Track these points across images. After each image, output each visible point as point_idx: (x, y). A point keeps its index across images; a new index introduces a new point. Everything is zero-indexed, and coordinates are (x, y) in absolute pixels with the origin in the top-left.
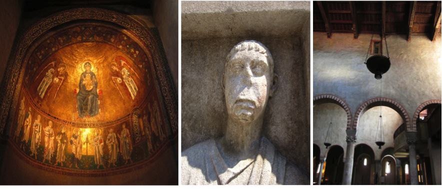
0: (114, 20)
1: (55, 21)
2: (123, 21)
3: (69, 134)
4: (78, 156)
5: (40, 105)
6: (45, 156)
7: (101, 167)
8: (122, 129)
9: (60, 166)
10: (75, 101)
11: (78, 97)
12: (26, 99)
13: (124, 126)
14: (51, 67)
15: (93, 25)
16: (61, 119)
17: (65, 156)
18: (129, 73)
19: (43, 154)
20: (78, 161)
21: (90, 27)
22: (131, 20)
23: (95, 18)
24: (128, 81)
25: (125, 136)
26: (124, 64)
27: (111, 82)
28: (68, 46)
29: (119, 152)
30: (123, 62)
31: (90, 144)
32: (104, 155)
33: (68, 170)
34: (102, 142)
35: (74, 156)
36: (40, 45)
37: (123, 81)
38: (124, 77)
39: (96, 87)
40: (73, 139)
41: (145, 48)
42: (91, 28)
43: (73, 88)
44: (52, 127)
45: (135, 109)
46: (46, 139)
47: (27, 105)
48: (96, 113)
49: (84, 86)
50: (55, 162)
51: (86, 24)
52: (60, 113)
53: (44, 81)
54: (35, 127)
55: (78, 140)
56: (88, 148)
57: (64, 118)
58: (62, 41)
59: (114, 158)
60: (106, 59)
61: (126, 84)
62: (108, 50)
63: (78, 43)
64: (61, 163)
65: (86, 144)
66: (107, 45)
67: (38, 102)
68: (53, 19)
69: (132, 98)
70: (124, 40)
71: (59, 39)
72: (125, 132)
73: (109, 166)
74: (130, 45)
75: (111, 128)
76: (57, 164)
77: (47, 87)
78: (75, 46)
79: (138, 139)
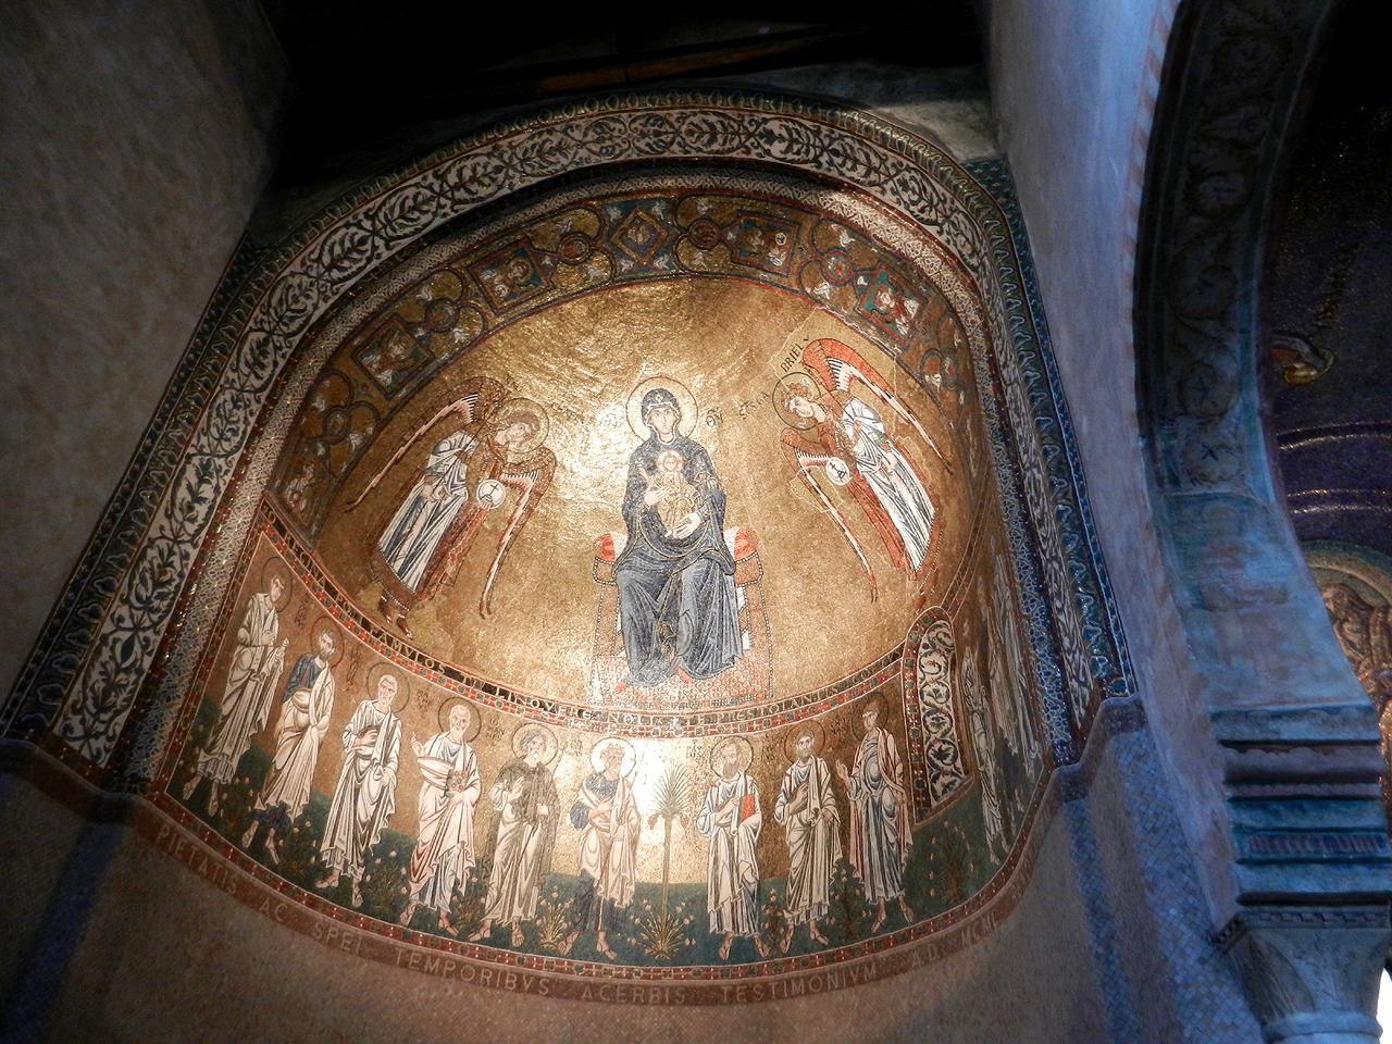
0: (777, 149)
1: (456, 187)
2: (824, 149)
3: (565, 773)
4: (616, 892)
5: (401, 624)
6: (415, 888)
7: (743, 949)
8: (861, 734)
9: (507, 945)
10: (609, 601)
11: (625, 576)
12: (291, 588)
13: (870, 718)
14: (453, 422)
15: (669, 190)
16: (524, 691)
17: (535, 891)
18: (880, 427)
19: (405, 881)
20: (615, 920)
21: (652, 201)
22: (864, 136)
23: (676, 151)
24: (884, 470)
25: (873, 770)
27: (796, 486)
28: (537, 311)
29: (845, 860)
30: (845, 372)
31: (684, 822)
33: (549, 966)
35: (592, 890)
36: (374, 315)
38: (859, 449)
39: (720, 520)
40: (587, 798)
41: (948, 274)
42: (657, 209)
43: (593, 533)
45: (929, 622)
46: (428, 799)
47: (298, 621)
49: (652, 516)
50: (475, 926)
51: (628, 187)
52: (518, 663)
54: (362, 734)
55: (618, 801)
56: (673, 846)
57: (543, 686)
60: (754, 361)
61: (877, 490)
62: (758, 313)
63: (594, 289)
65: (661, 821)
66: (755, 289)
67: (383, 608)
68: (441, 177)
69: (909, 559)
70: (837, 250)
71: (486, 277)
72: (877, 747)
73: (785, 946)
74: (871, 274)
75: (805, 729)
77: (441, 528)
78: (578, 309)
79: (946, 787)
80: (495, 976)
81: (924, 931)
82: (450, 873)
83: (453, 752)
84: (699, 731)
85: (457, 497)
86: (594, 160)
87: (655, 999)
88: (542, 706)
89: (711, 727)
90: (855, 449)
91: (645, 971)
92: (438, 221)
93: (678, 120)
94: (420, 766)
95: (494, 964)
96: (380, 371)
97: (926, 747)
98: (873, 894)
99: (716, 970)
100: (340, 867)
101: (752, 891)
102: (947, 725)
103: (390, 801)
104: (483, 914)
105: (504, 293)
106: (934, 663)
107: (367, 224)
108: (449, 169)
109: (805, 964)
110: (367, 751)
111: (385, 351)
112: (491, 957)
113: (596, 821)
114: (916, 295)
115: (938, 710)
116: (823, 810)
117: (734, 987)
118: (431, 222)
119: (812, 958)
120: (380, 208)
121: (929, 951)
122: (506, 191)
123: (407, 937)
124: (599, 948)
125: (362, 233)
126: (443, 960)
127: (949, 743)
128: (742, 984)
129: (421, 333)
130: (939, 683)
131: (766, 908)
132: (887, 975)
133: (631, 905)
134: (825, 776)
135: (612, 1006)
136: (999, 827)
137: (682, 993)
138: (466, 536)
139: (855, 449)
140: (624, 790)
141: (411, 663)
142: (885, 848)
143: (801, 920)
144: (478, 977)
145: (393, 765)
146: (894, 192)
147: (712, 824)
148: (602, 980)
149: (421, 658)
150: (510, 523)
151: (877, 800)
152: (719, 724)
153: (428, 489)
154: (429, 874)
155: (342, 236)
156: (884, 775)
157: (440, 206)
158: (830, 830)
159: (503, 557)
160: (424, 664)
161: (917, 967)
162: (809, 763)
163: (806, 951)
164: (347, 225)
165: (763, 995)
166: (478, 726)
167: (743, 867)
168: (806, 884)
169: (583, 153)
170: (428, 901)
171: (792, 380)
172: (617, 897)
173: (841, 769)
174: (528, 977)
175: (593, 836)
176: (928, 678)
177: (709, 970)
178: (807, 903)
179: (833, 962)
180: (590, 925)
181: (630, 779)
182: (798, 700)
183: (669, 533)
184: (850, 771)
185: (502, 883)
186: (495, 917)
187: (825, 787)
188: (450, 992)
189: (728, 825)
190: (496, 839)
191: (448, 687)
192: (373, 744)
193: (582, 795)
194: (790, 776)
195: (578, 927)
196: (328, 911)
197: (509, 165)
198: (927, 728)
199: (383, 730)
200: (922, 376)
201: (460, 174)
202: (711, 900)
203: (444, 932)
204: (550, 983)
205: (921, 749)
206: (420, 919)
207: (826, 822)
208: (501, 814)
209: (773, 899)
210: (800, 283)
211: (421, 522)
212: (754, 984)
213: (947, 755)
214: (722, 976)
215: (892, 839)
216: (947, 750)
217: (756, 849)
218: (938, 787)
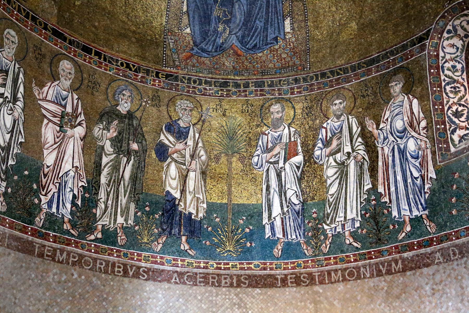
8: (388, 98)
9: (114, 243)
19: (36, 194)
25: (399, 125)
31: (242, 159)
32: (303, 203)
34: (297, 154)
44: (73, 89)
48: (271, 36)
50: (90, 229)
55: (190, 142)
80: (107, 265)
81: (448, 238)
82: (69, 190)
83: (64, 97)
87: (226, 283)
88: (128, 66)
89: (261, 90)
91: (217, 264)
94: (41, 106)
95: (106, 257)
97: (446, 108)
98: (399, 212)
99: (271, 264)
101: (297, 211)
102: (462, 93)
103: (20, 131)
106: (453, 46)
109: (342, 260)
112: (103, 251)
113: (175, 156)
115: (455, 81)
116: (355, 154)
117: (286, 275)
119: (347, 256)
121: (451, 253)
124: (182, 247)
127: (464, 106)
128: (292, 274)
130: (456, 61)
131: (309, 222)
132: (411, 269)
134: (356, 129)
135: (195, 288)
137: (246, 279)
140: (194, 135)
141: (27, 22)
142: (409, 180)
143: (338, 230)
144: (95, 265)
145: (20, 104)
147: (264, 161)
148: (186, 270)
149: (34, 19)
151: (402, 147)
152: (266, 88)
154: (53, 189)
156: (409, 128)
158: (361, 167)
160: (36, 24)
162: (342, 118)
163: (342, 252)
165: (308, 282)
166: (81, 79)
167: (290, 193)
170: (54, 210)
172: (194, 212)
173: (371, 126)
174: (132, 267)
175: (173, 167)
176: (448, 57)
177: (265, 264)
178: (343, 219)
179: (365, 259)
180: (175, 231)
181: (199, 126)
184: (378, 125)
185: (108, 199)
186: (104, 223)
187: (355, 137)
188: (76, 276)
189: (277, 162)
190: (101, 165)
191: (56, 45)
193: (162, 137)
194: (326, 129)
195: (166, 232)
198: (447, 94)
202: (265, 215)
203: (68, 232)
205: (443, 110)
206: (50, 222)
207: (356, 162)
208: (103, 147)
209: (315, 215)
212: (301, 274)
213: (462, 115)
214: (276, 268)
215: (416, 174)
216: (462, 111)
217: (300, 180)
218: (456, 138)
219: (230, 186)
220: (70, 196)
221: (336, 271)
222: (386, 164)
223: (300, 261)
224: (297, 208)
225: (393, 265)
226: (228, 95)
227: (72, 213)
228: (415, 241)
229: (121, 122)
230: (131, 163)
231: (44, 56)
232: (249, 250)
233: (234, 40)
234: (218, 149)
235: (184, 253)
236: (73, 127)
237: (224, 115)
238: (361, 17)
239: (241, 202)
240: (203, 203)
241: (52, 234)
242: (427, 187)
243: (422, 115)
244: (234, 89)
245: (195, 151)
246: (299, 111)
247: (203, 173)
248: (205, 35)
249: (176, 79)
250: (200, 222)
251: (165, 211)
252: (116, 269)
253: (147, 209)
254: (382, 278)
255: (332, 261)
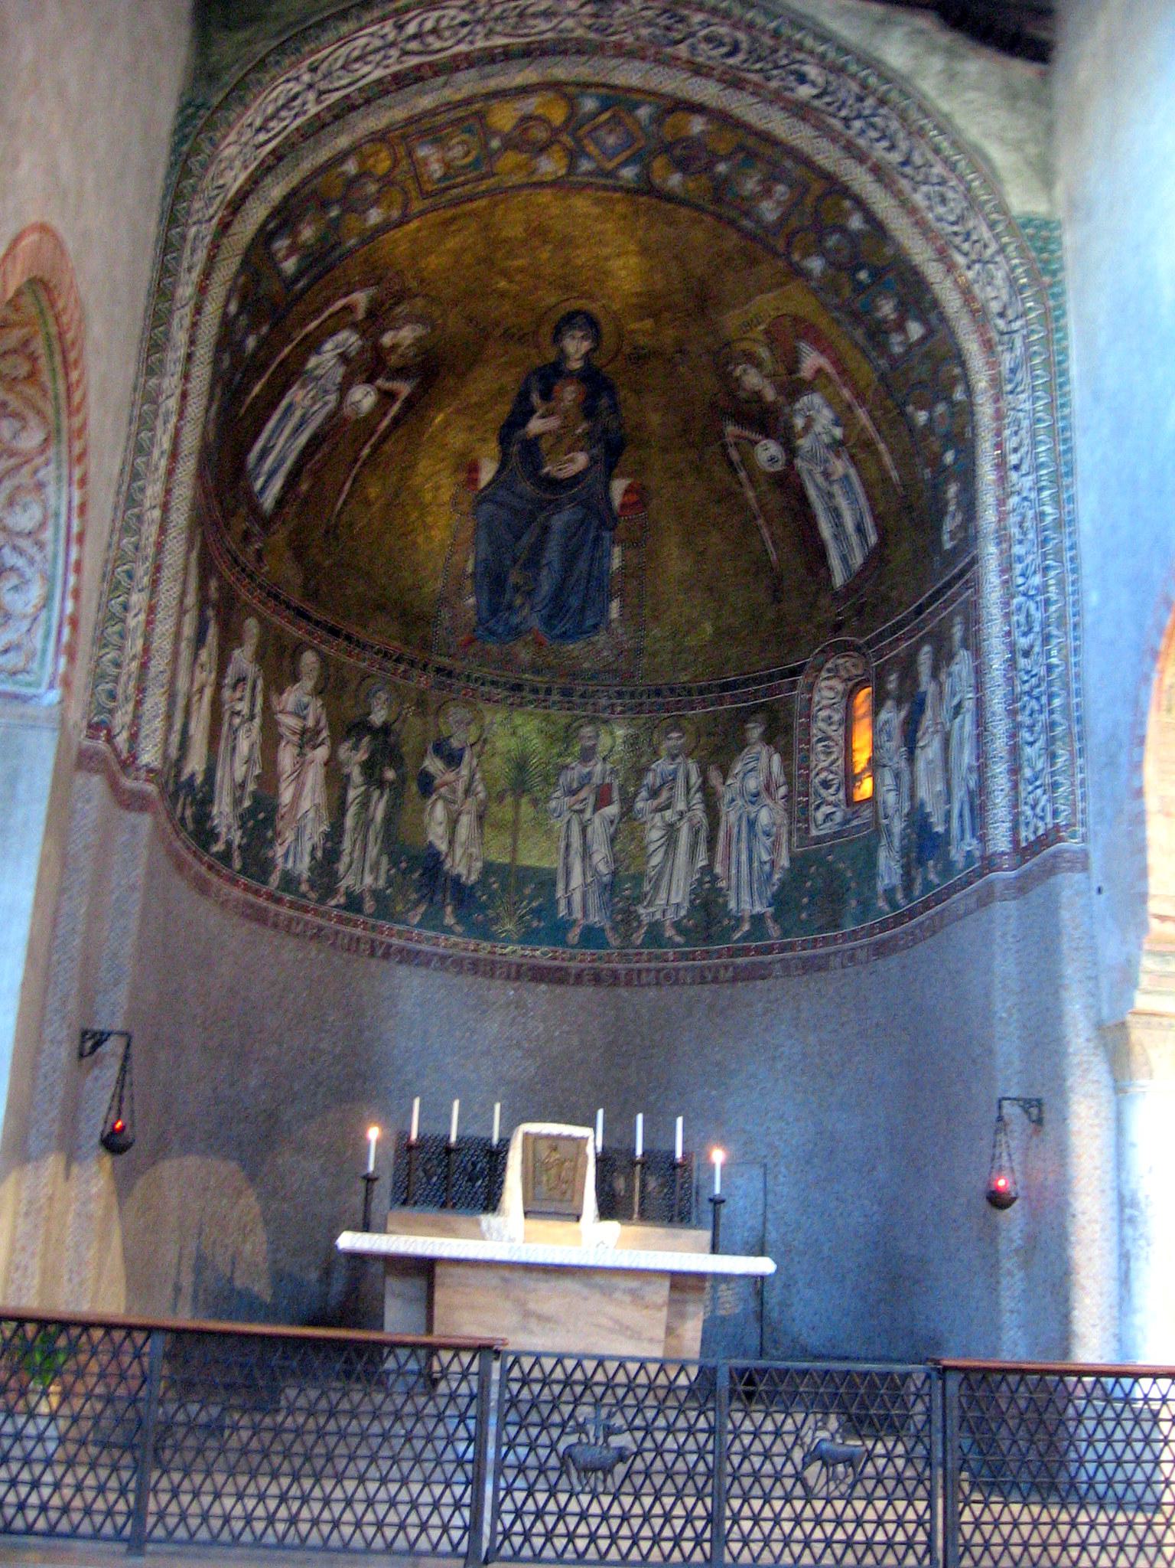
0: (804, 92)
2: (858, 117)
3: (412, 732)
6: (280, 851)
7: (592, 937)
8: (742, 744)
9: (359, 910)
11: (488, 508)
13: (755, 731)
14: (343, 319)
17: (385, 860)
18: (838, 432)
19: (271, 843)
21: (637, 105)
24: (826, 475)
25: (752, 784)
26: (819, 371)
29: (708, 869)
30: (812, 361)
31: (535, 802)
34: (610, 803)
36: (294, 192)
37: (790, 463)
38: (805, 443)
40: (433, 764)
44: (318, 692)
48: (589, 623)
50: (330, 891)
53: (290, 406)
54: (234, 687)
55: (465, 771)
58: (436, 169)
59: (674, 900)
61: (812, 493)
64: (361, 897)
65: (509, 799)
67: (247, 537)
68: (400, 27)
70: (843, 230)
71: (422, 152)
73: (638, 938)
74: (877, 274)
76: (342, 900)
77: (303, 439)
79: (828, 817)
81: (791, 947)
84: (554, 703)
85: (326, 404)
86: (579, 32)
90: (800, 442)
92: (378, 74)
93: (701, 23)
95: (349, 929)
96: (286, 257)
100: (224, 830)
104: (337, 880)
105: (438, 175)
106: (831, 688)
107: (306, 78)
108: (408, 22)
109: (657, 958)
110: (239, 707)
111: (295, 234)
114: (925, 322)
117: (583, 970)
118: (369, 73)
120: (323, 61)
122: (463, 48)
123: (279, 901)
125: (298, 88)
126: (307, 923)
129: (334, 213)
133: (478, 882)
134: (695, 780)
136: (896, 880)
138: (326, 448)
139: (800, 442)
142: (756, 864)
146: (928, 197)
148: (451, 952)
150: (371, 435)
151: (753, 815)
152: (576, 699)
153: (301, 393)
155: (282, 90)
156: (764, 794)
157: (386, 57)
159: (357, 475)
161: (777, 977)
162: (678, 760)
163: (660, 947)
164: (288, 81)
167: (597, 858)
168: (664, 883)
169: (569, 23)
170: (290, 865)
171: (745, 345)
173: (715, 777)
174: (382, 943)
176: (825, 702)
180: (438, 897)
181: (477, 748)
182: (672, 690)
183: (546, 470)
184: (725, 778)
189: (582, 811)
192: (241, 699)
193: (427, 763)
196: (218, 873)
197: (480, 21)
199: (249, 683)
200: (905, 404)
201: (421, 24)
202: (561, 886)
204: (401, 950)
207: (692, 827)
208: (348, 776)
210: (789, 244)
211: (287, 432)
217: (613, 840)
218: (820, 815)
219: (515, 841)
220: (308, 847)
221: (648, 970)
222: (729, 835)
223: (602, 952)
224: (606, 879)
225: (722, 972)
226: (521, 705)
227: (310, 869)
228: (754, 944)
229: (374, 738)
230: (385, 797)
231: (284, 648)
232: (537, 931)
233: (535, 622)
234: (502, 784)
235: (448, 930)
236: (314, 748)
237: (514, 733)
238: (719, 617)
239: (528, 862)
240: (477, 859)
241: (288, 897)
242: (777, 876)
243: (782, 779)
244: (532, 697)
245: (470, 785)
246: (619, 741)
247: (481, 818)
248: (494, 611)
249: (450, 674)
250: (473, 887)
251: (426, 870)
252: (362, 946)
253: (403, 865)
254: (706, 987)
255: (645, 957)
